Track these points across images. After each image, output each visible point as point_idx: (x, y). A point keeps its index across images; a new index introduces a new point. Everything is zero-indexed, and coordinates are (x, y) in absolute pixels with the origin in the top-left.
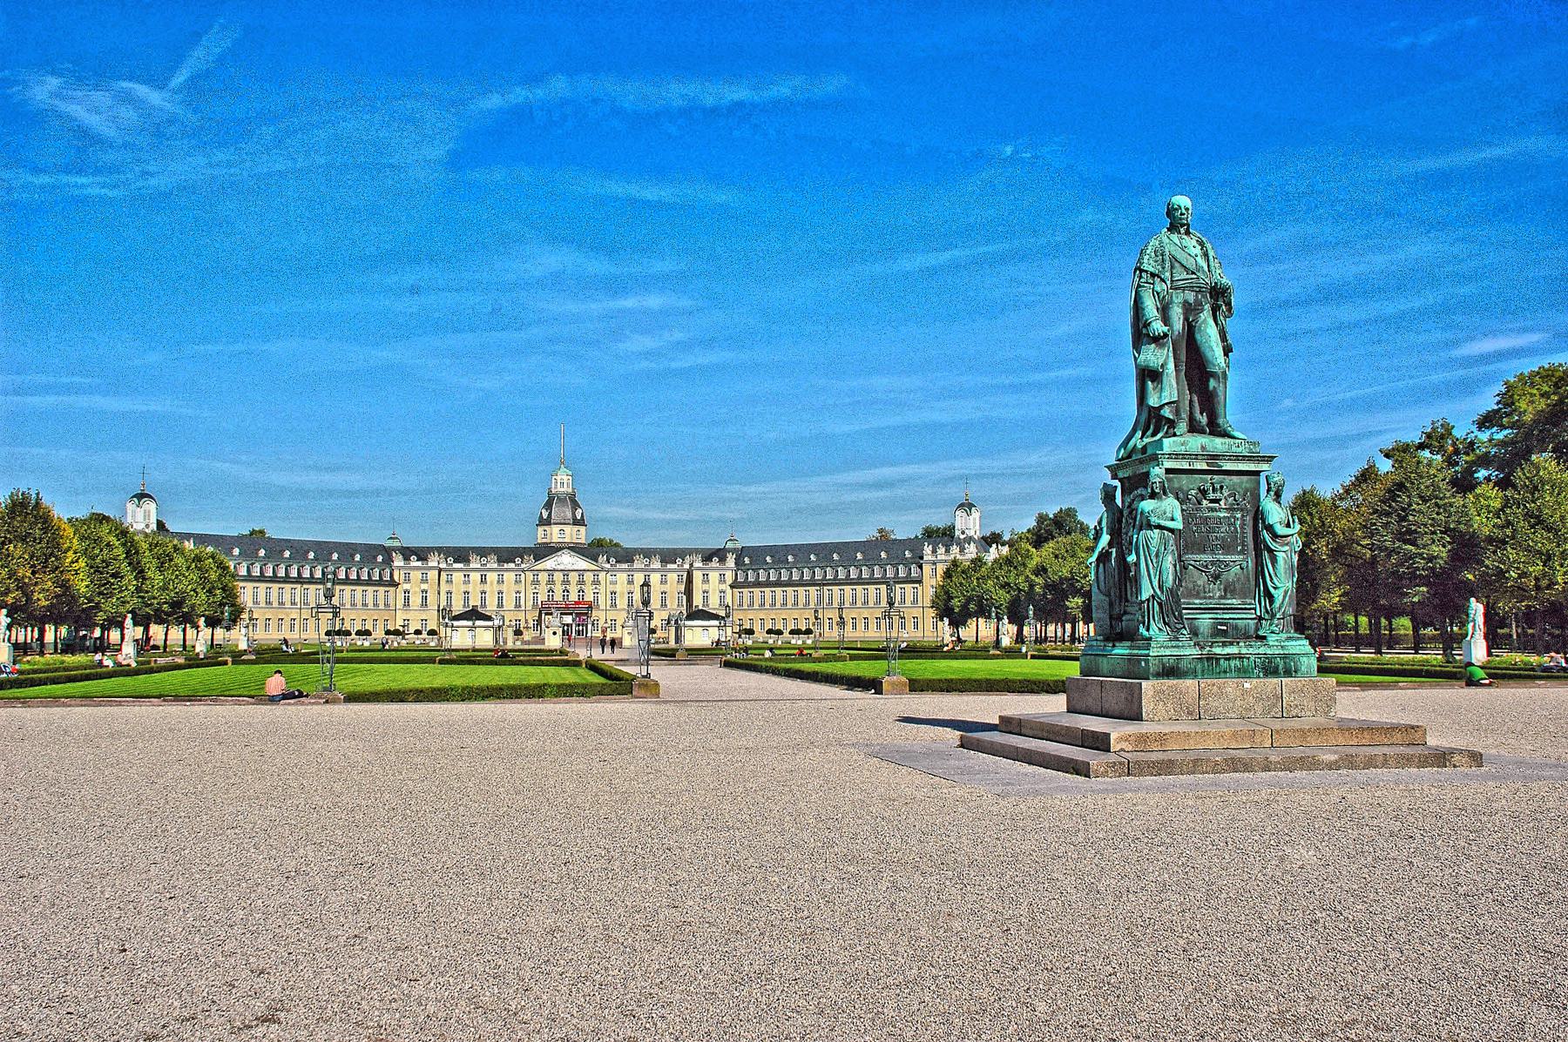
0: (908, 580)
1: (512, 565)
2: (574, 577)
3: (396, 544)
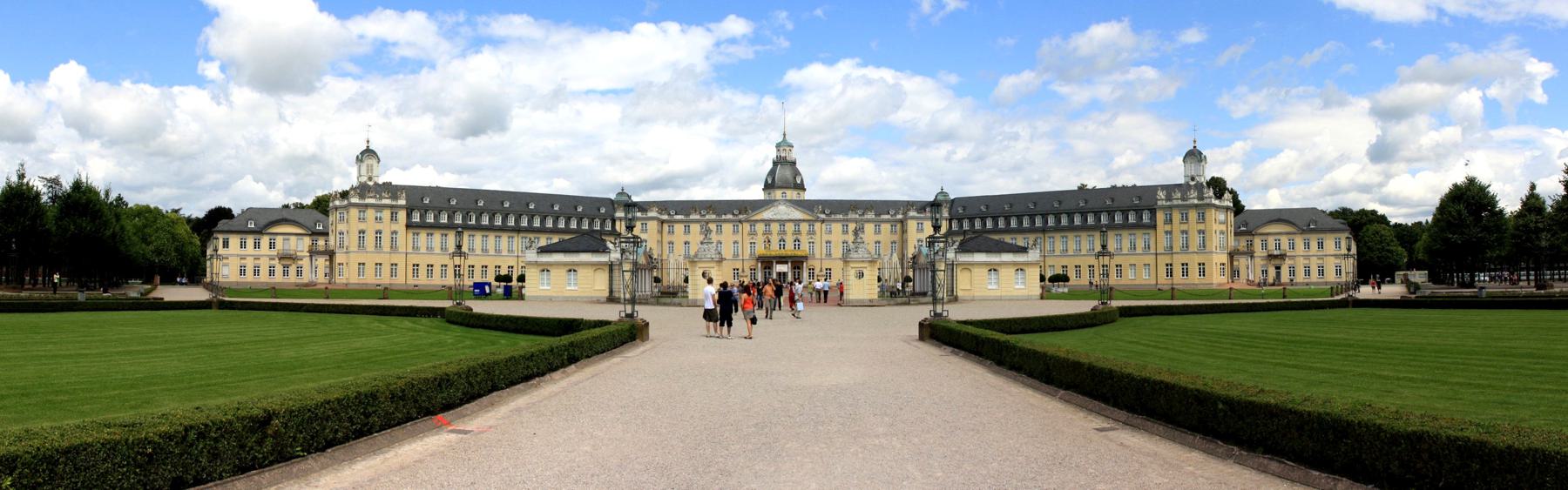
0: (1139, 226)
1: (730, 216)
2: (790, 227)
3: (625, 198)
